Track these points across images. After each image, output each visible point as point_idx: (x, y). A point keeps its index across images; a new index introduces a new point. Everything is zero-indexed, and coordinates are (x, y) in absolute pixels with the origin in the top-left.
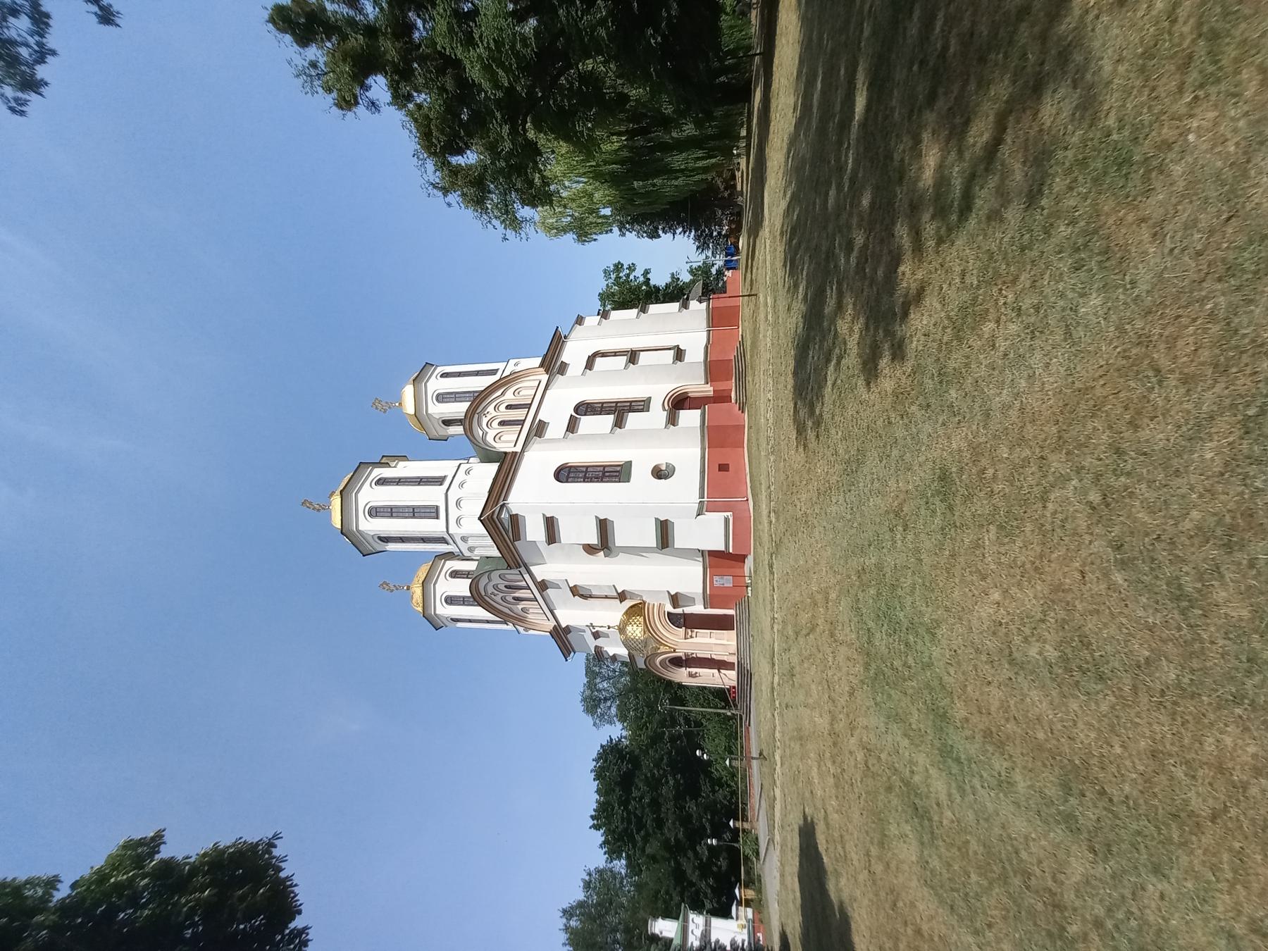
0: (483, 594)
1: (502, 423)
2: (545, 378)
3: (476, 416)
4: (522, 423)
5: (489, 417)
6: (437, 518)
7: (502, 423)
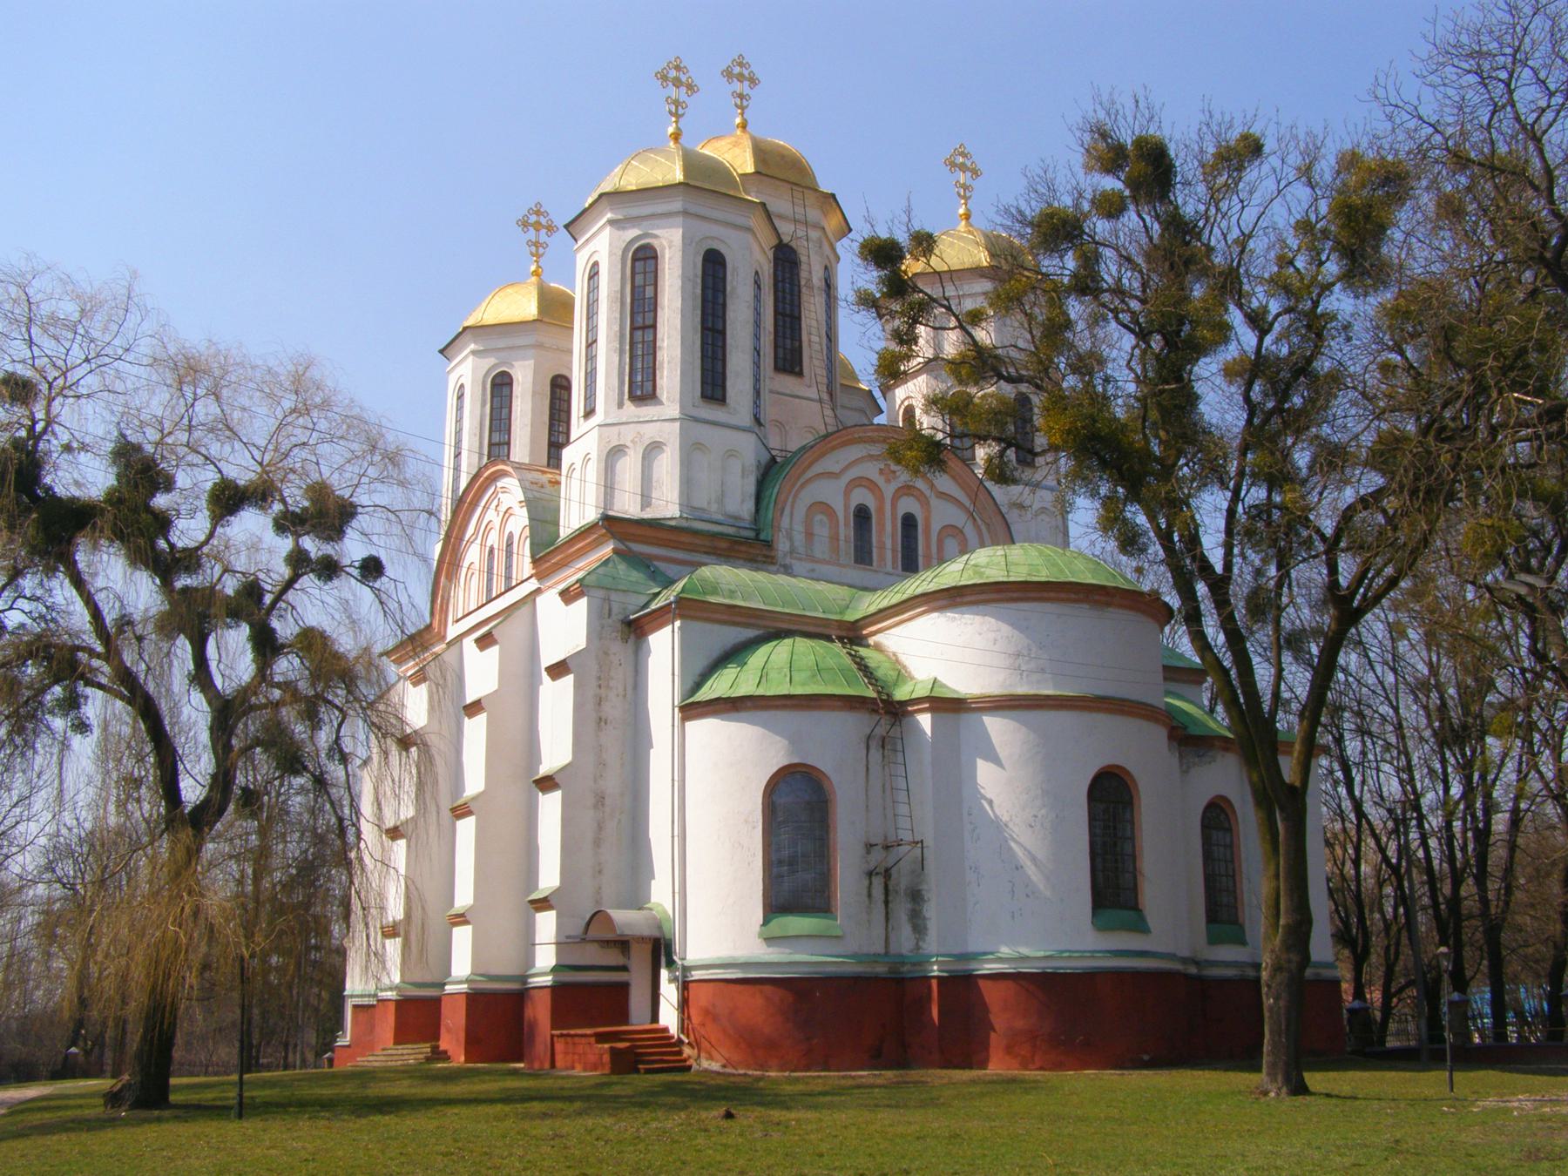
0: (499, 484)
1: (862, 516)
5: (880, 481)
6: (634, 398)
7: (862, 516)
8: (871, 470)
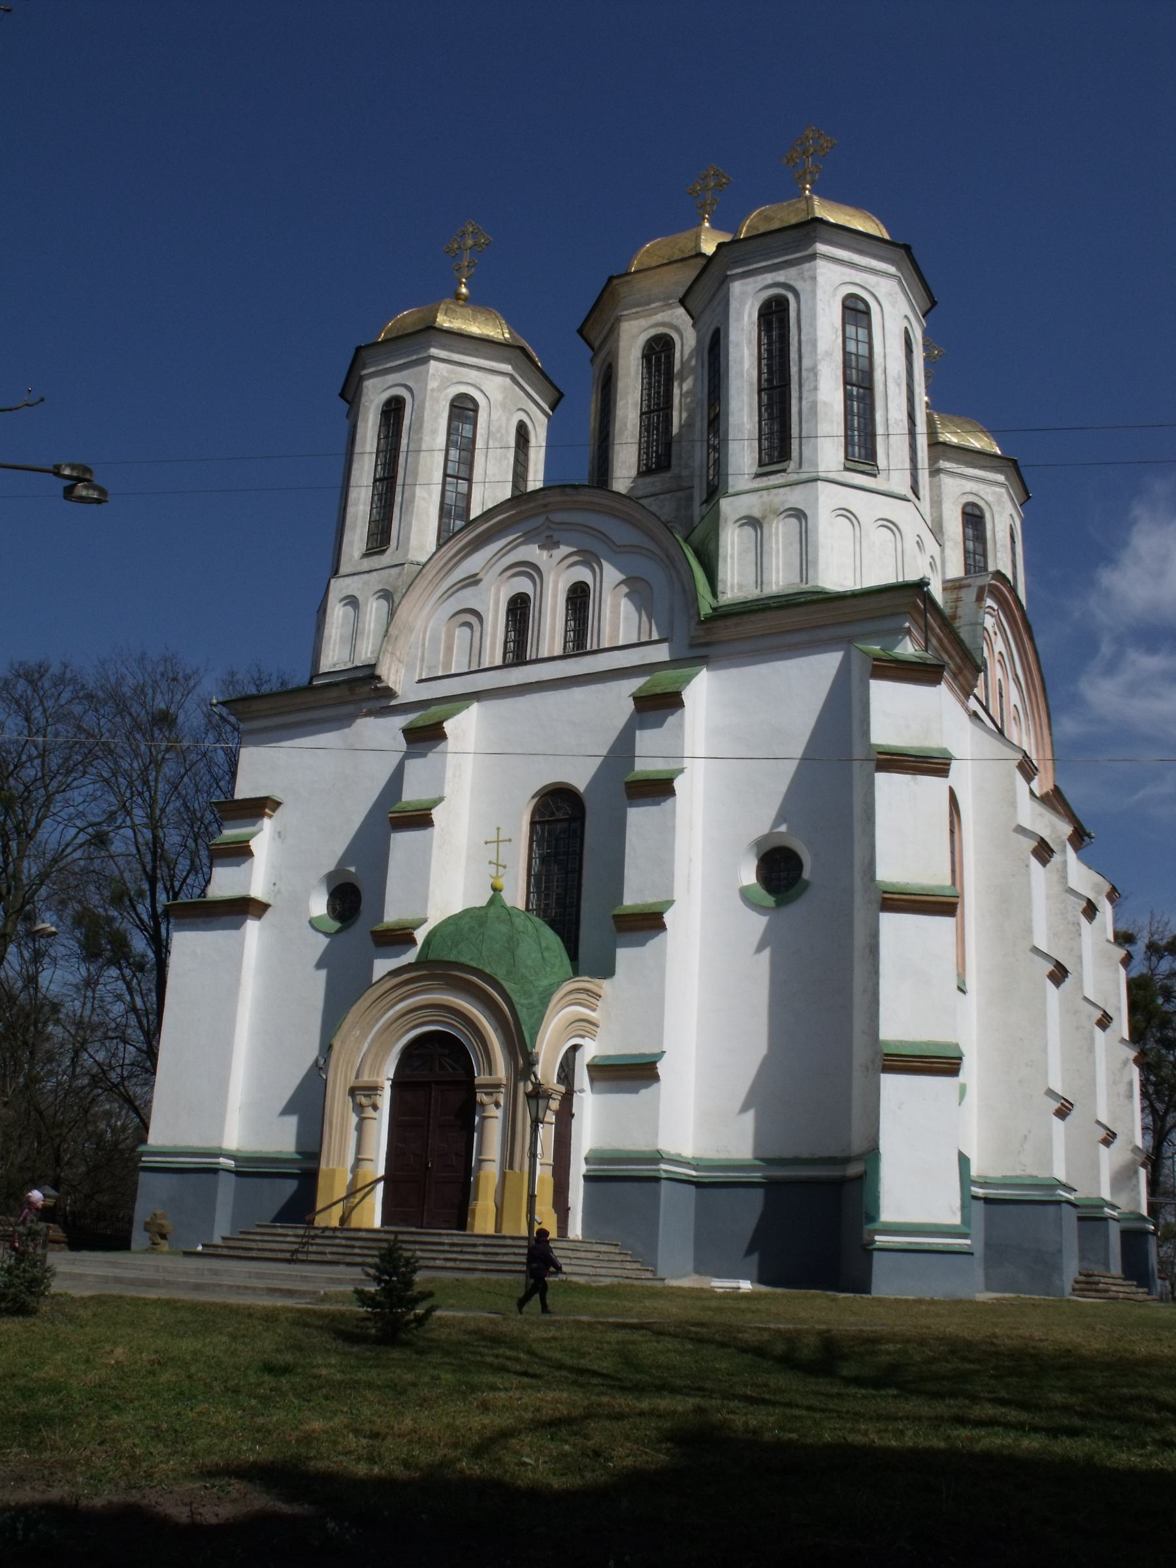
7: (519, 608)
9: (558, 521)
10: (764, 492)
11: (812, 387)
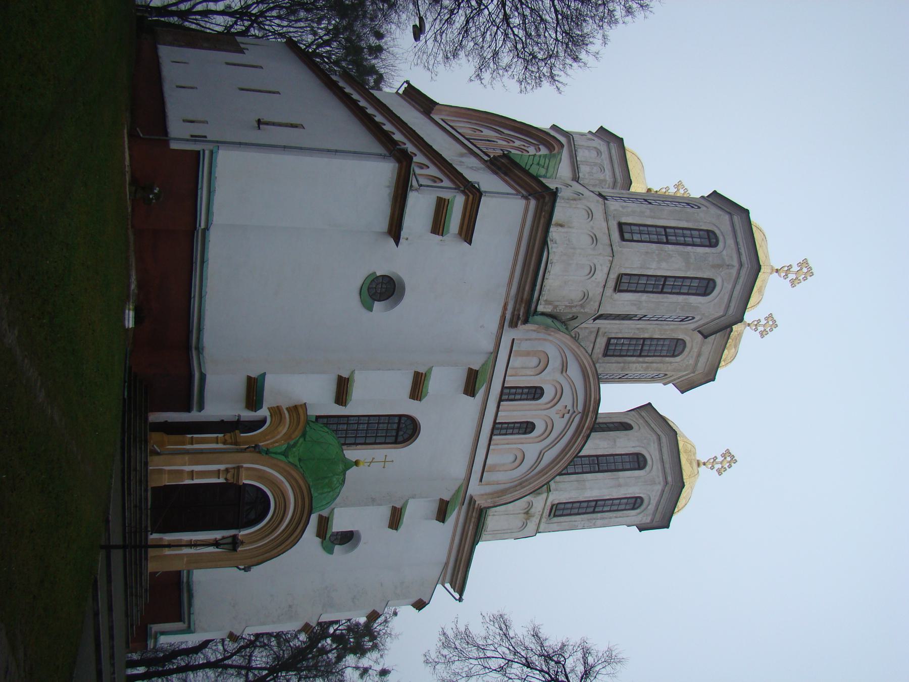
0: (541, 147)
1: (535, 393)
2: (474, 489)
3: (580, 408)
4: (509, 394)
5: (559, 406)
7: (535, 393)
8: (567, 400)
9: (575, 420)
10: (541, 513)
11: (585, 525)
